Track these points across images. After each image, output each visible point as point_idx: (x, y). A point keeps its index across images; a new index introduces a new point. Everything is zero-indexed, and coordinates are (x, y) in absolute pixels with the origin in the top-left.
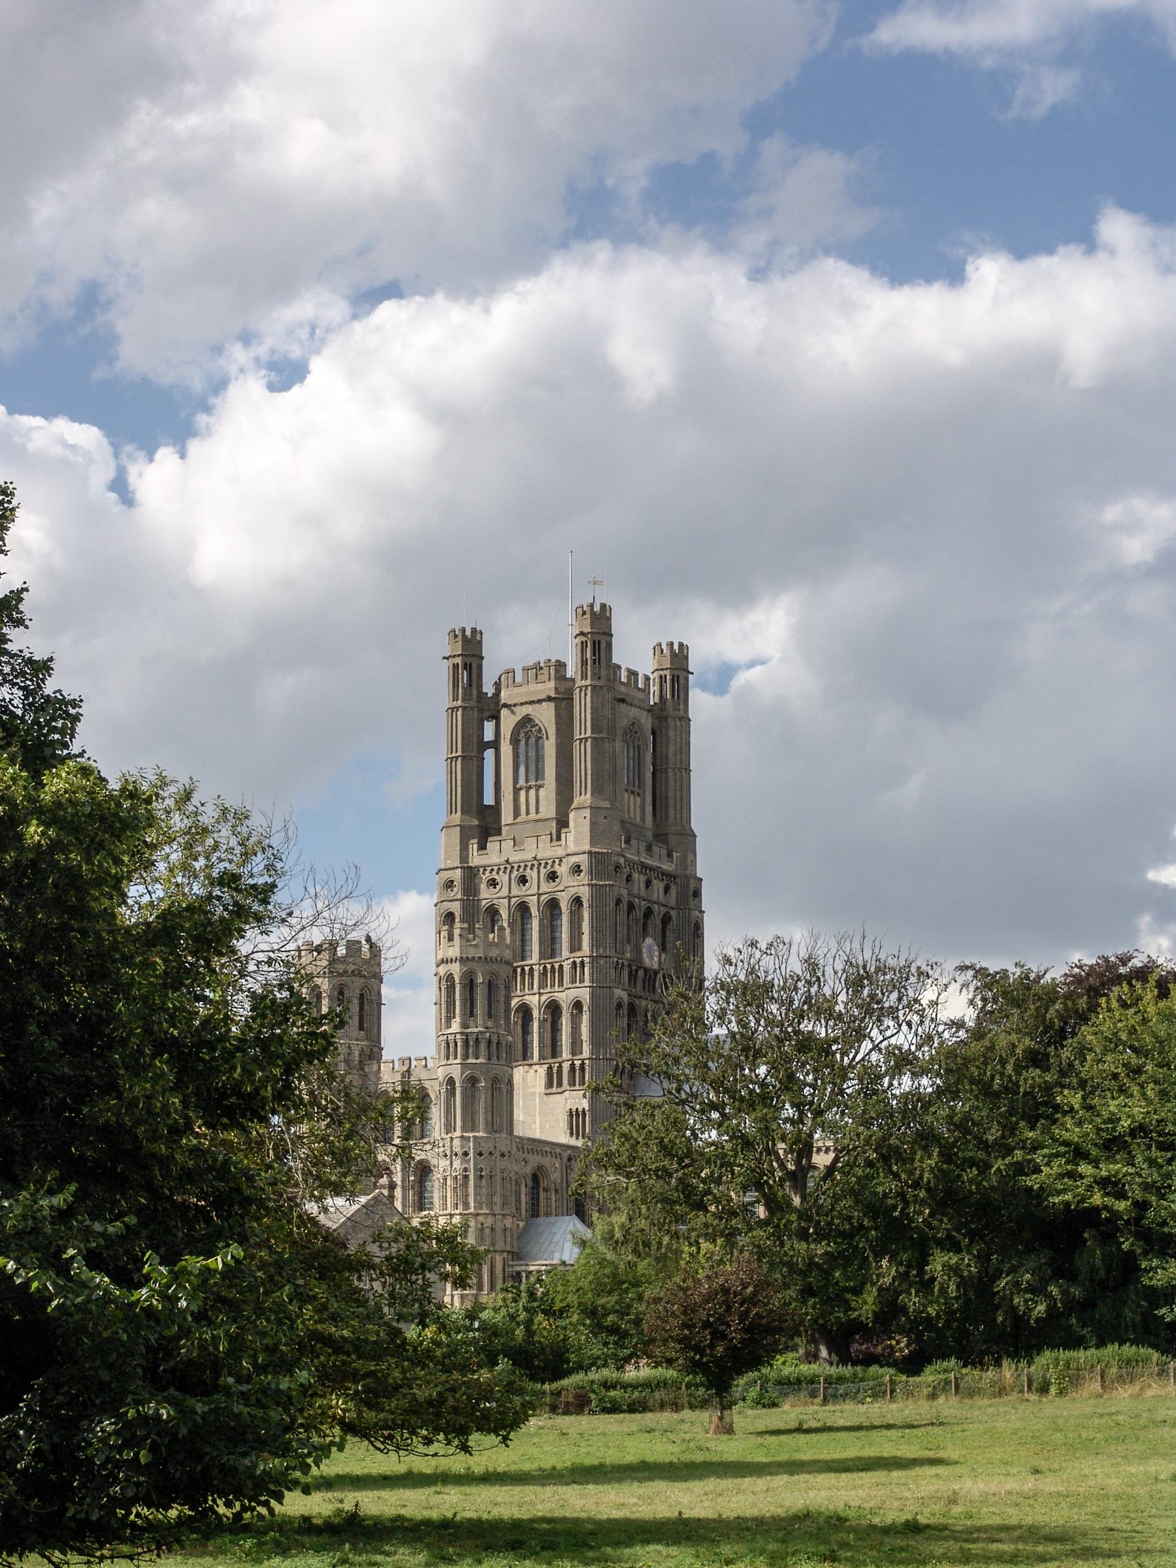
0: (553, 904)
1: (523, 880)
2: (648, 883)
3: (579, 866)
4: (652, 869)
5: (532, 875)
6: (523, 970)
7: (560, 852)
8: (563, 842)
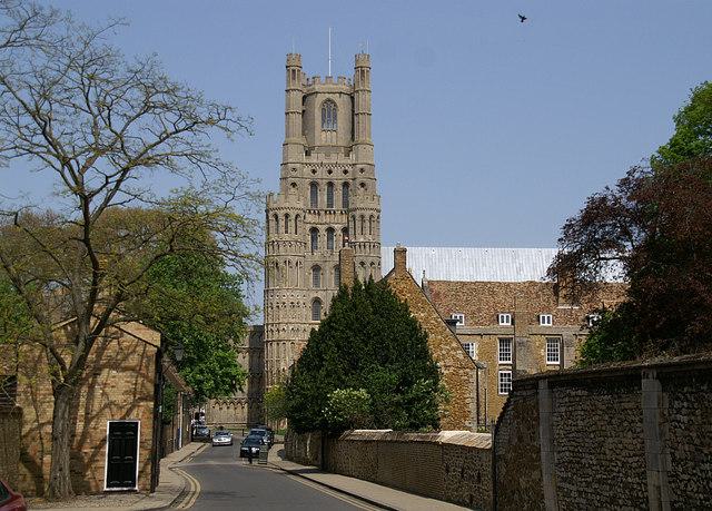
5: (335, 170)
7: (349, 162)
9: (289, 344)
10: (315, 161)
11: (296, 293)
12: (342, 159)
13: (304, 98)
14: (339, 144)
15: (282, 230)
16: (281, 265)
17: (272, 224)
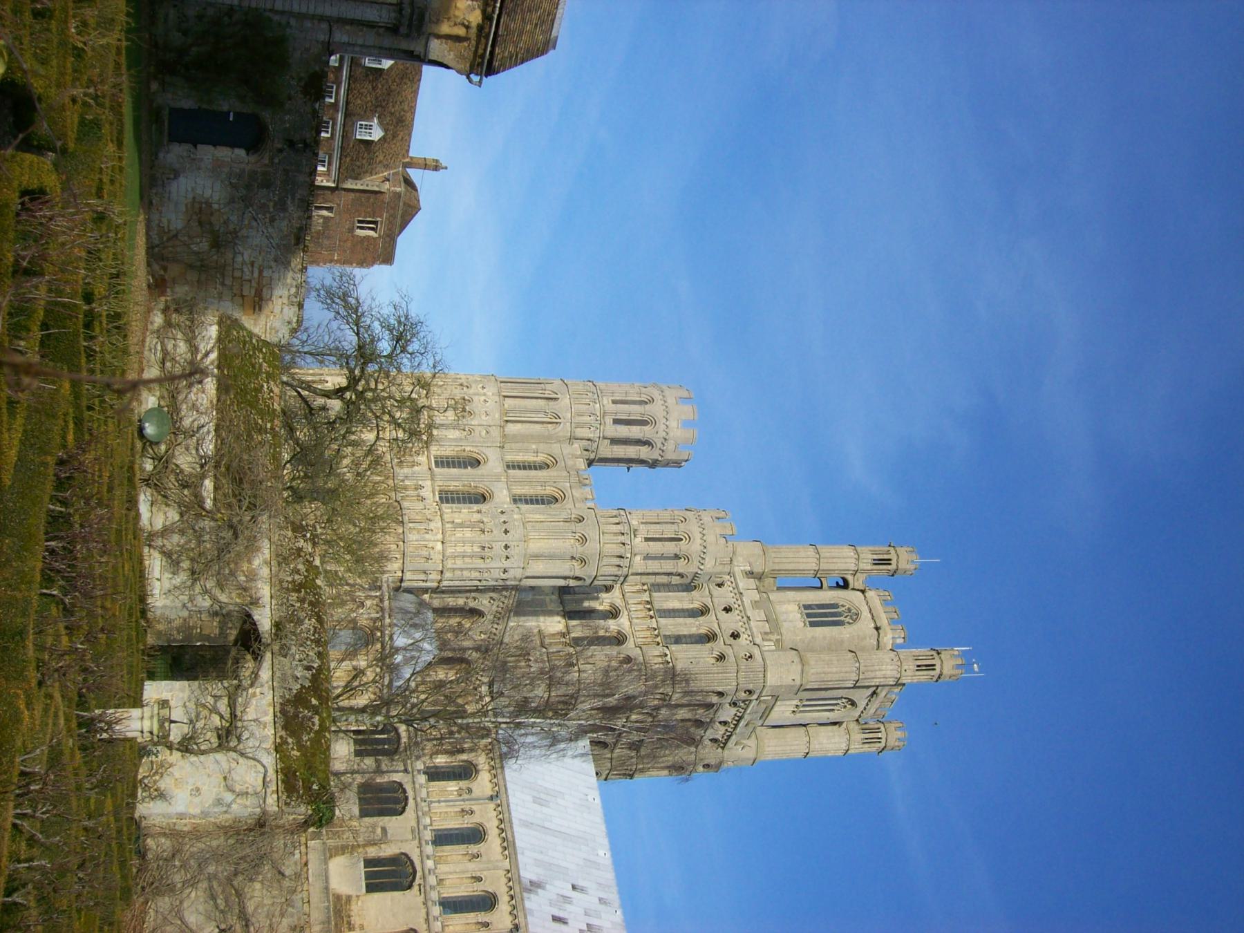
0: (709, 638)
1: (727, 610)
2: (725, 723)
3: (750, 657)
4: (736, 725)
6: (650, 610)
7: (758, 640)
8: (766, 643)
10: (741, 585)
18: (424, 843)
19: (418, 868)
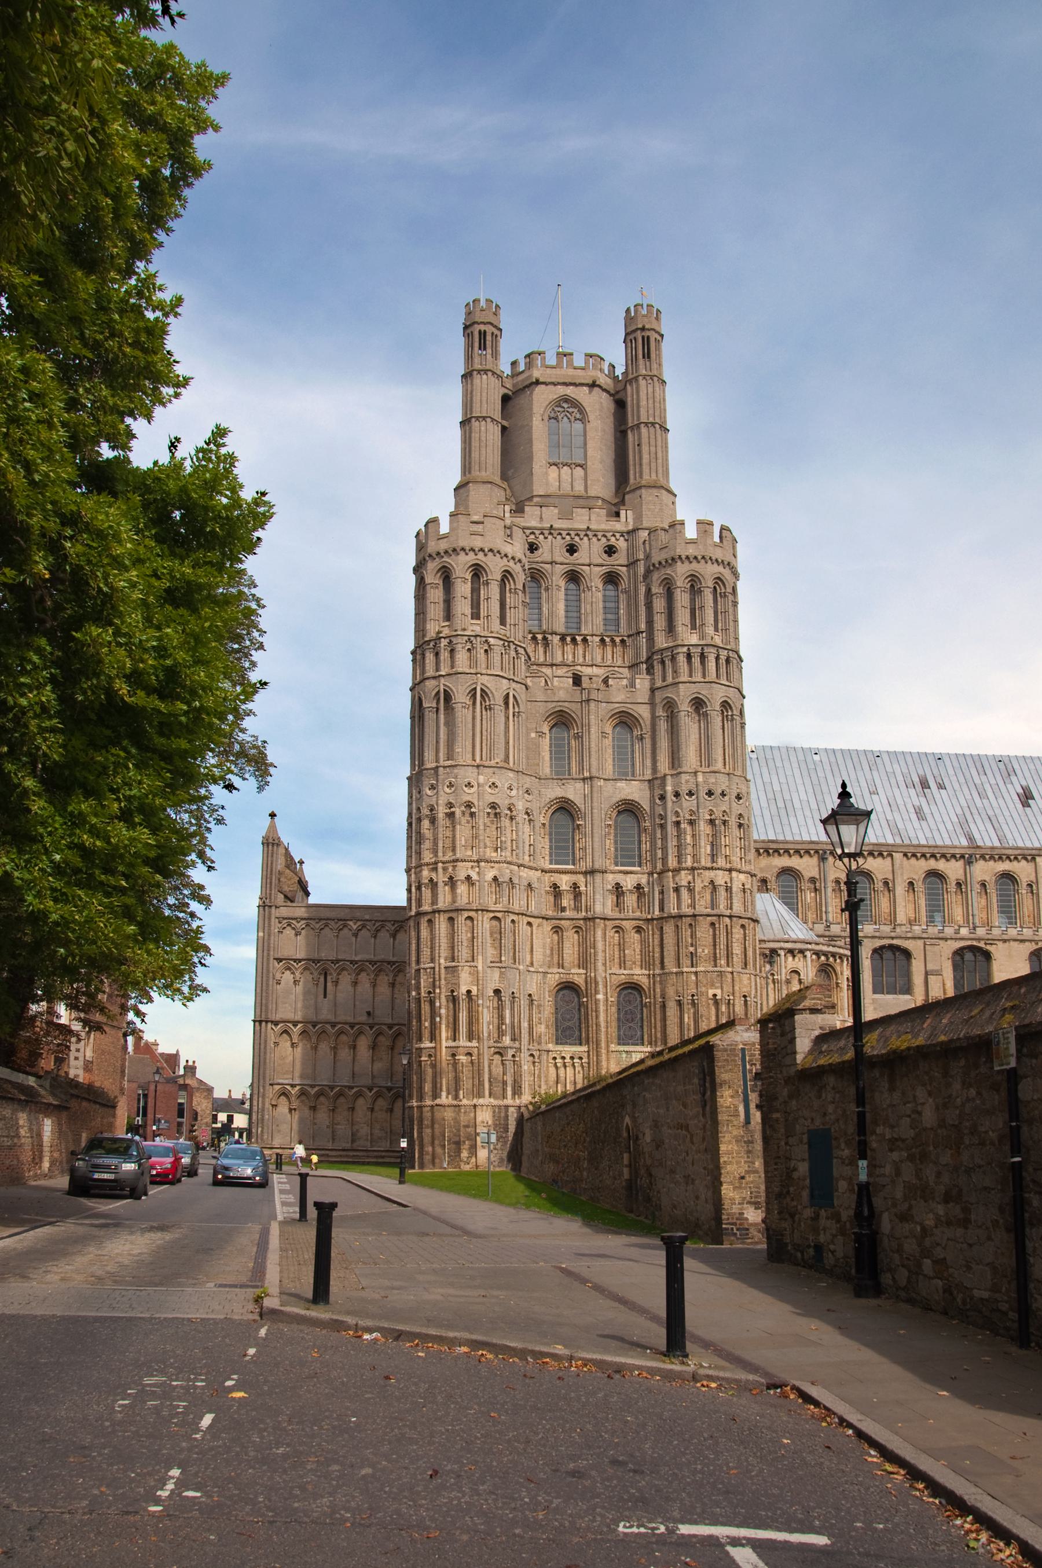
1: (572, 549)
9: (484, 924)
10: (534, 523)
11: (504, 779)
12: (599, 520)
13: (506, 399)
14: (592, 493)
15: (462, 607)
16: (461, 697)
17: (435, 595)
18: (941, 935)
19: (969, 943)
